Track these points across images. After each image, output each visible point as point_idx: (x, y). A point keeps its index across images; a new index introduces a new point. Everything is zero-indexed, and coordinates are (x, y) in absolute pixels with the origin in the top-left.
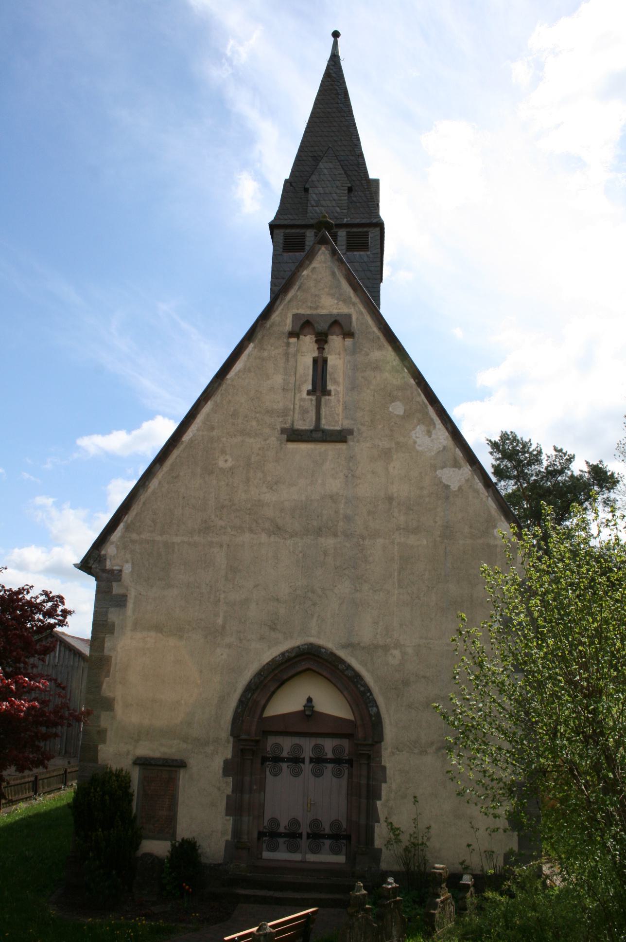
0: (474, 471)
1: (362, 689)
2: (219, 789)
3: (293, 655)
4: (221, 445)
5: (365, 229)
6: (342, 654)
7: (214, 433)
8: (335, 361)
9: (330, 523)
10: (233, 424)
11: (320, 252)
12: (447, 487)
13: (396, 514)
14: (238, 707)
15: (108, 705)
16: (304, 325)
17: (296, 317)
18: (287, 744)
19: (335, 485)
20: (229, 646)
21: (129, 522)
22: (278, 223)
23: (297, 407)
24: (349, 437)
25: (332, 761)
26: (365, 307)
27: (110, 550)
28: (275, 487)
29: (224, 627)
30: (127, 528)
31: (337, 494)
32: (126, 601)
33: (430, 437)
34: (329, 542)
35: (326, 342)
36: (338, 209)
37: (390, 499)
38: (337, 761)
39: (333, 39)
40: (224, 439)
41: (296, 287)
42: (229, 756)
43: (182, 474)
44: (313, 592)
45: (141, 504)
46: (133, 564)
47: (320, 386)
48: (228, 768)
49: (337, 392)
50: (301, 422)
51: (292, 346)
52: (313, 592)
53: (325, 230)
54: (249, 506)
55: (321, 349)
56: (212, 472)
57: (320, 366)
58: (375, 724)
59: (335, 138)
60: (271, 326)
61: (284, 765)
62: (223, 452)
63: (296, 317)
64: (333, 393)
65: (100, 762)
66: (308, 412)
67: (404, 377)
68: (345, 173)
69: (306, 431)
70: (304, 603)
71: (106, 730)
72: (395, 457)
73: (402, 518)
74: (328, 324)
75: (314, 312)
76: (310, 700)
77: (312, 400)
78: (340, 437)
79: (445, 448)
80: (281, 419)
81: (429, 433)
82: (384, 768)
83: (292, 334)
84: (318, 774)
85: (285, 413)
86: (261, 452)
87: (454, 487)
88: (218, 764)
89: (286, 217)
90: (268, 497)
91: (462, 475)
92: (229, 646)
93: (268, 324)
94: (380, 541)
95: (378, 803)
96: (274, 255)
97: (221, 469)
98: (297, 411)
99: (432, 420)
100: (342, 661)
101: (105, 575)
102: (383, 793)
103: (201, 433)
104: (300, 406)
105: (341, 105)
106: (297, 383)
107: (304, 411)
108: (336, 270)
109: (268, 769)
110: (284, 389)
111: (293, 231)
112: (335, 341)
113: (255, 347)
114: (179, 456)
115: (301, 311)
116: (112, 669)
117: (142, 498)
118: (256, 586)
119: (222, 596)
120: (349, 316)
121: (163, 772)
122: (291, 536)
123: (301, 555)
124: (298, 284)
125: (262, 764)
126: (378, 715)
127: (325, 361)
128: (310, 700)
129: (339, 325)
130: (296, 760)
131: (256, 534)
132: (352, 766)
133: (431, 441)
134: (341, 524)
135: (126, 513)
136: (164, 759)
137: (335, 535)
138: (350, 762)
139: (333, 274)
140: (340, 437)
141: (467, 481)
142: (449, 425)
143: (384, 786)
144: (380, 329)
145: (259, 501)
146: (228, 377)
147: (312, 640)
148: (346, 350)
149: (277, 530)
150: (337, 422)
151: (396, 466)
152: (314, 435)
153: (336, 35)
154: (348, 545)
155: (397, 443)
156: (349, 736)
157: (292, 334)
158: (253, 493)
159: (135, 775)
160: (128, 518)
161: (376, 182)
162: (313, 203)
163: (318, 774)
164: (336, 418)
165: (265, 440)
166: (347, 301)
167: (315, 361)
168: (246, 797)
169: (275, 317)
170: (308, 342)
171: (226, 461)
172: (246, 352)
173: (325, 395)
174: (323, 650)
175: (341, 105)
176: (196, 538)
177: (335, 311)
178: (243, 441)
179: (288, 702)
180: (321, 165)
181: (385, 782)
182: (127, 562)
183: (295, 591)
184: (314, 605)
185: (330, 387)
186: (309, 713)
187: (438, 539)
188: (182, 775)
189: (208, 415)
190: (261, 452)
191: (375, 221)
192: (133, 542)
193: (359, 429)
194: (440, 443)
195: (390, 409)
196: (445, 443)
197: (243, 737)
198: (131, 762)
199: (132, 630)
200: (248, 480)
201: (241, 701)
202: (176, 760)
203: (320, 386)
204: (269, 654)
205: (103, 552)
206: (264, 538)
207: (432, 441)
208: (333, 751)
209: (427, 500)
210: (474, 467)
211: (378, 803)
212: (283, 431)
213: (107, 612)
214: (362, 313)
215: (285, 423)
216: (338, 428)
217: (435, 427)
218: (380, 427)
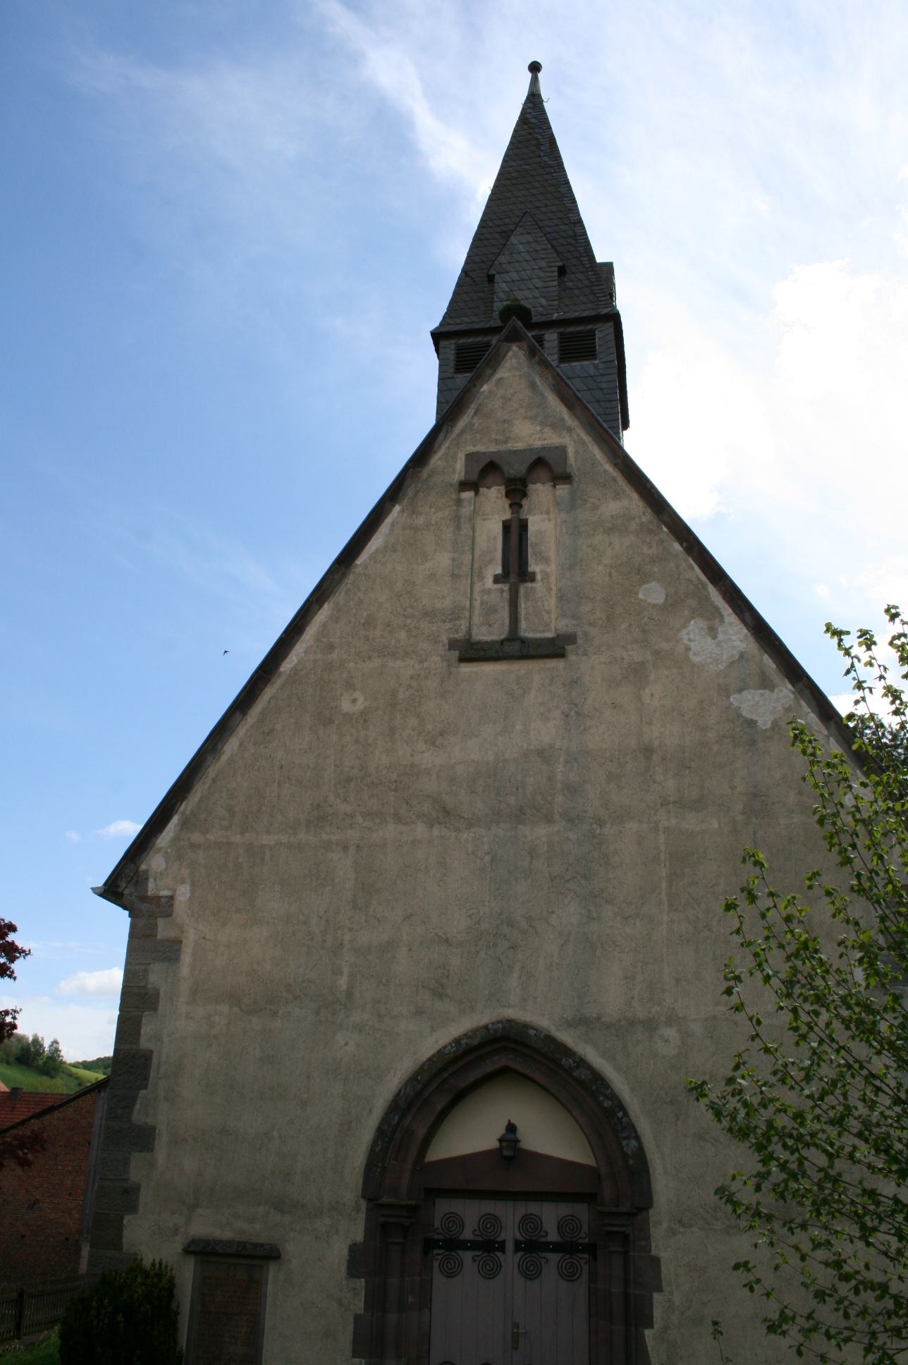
0: (800, 692)
1: (607, 1104)
2: (340, 1303)
3: (476, 1042)
4: (345, 675)
5: (589, 327)
6: (566, 1037)
7: (334, 656)
8: (543, 524)
9: (539, 798)
10: (367, 639)
11: (510, 353)
12: (751, 723)
13: (659, 778)
14: (375, 1143)
15: (144, 1139)
16: (486, 471)
17: (470, 457)
18: (471, 1214)
19: (546, 732)
20: (359, 1028)
21: (188, 813)
22: (446, 329)
23: (477, 604)
24: (569, 648)
25: (556, 1247)
26: (588, 433)
27: (155, 862)
28: (439, 741)
29: (349, 994)
30: (185, 824)
31: (551, 746)
32: (179, 950)
33: (714, 637)
34: (541, 832)
35: (524, 494)
36: (544, 302)
37: (647, 751)
38: (566, 1247)
39: (530, 75)
40: (351, 664)
41: (471, 411)
42: (360, 1237)
43: (279, 727)
44: (511, 924)
45: (209, 782)
46: (193, 884)
47: (516, 568)
48: (358, 1261)
49: (546, 575)
50: (484, 629)
51: (466, 504)
52: (511, 924)
53: (519, 323)
54: (394, 776)
55: (516, 506)
56: (331, 721)
57: (515, 533)
58: (636, 1171)
59: (537, 204)
60: (429, 476)
61: (467, 1256)
62: (350, 686)
63: (470, 457)
64: (539, 577)
65: (125, 1247)
66: (496, 611)
67: (662, 541)
68: (553, 247)
69: (493, 643)
70: (495, 945)
71: (139, 1186)
72: (652, 677)
73: (671, 783)
74: (526, 465)
75: (503, 448)
76: (511, 1128)
77: (502, 591)
78: (555, 649)
79: (742, 655)
80: (448, 625)
81: (712, 632)
82: (656, 1261)
83: (464, 485)
84: (531, 1273)
85: (455, 614)
86: (414, 684)
87: (764, 722)
88: (338, 1252)
89: (458, 321)
90: (430, 759)
91: (777, 700)
92: (359, 1028)
93: (425, 473)
94: (633, 826)
95: (648, 1333)
96: (441, 379)
97: (345, 715)
98: (476, 612)
99: (717, 609)
100: (568, 1052)
101: (144, 907)
102: (657, 1314)
103: (311, 657)
104: (482, 603)
105: (546, 159)
106: (476, 566)
107: (490, 610)
108: (537, 380)
109: (436, 1264)
110: (453, 576)
111: (471, 340)
112: (541, 492)
113: (403, 511)
114: (274, 697)
115: (480, 448)
116: (152, 1074)
117: (212, 771)
118: (408, 917)
119: (347, 937)
120: (563, 449)
121: (239, 1267)
122: (470, 826)
123: (487, 858)
124: (473, 406)
125: (426, 1253)
126: (640, 1154)
127: (524, 525)
128: (511, 1128)
129: (547, 466)
130: (488, 1246)
131: (407, 824)
132: (595, 1258)
133: (716, 646)
134: (560, 799)
135: (184, 798)
136: (239, 1243)
137: (549, 820)
138: (592, 1249)
139: (533, 386)
140: (555, 649)
141: (788, 710)
142: (748, 616)
143: (657, 1298)
144: (615, 465)
145: (412, 765)
146: (358, 562)
147: (511, 1013)
148: (558, 504)
149: (444, 814)
150: (547, 625)
151: (656, 693)
152: (506, 648)
153: (535, 68)
154: (572, 836)
155: (657, 653)
156: (589, 1198)
157: (464, 485)
158: (400, 753)
159: (186, 1275)
160: (186, 807)
161: (609, 267)
162: (502, 295)
163: (531, 1273)
164: (546, 617)
165: (422, 662)
166: (557, 425)
167: (506, 527)
168: (392, 1318)
169: (436, 460)
170: (494, 502)
171: (355, 701)
172: (388, 521)
173: (524, 581)
174: (532, 1032)
175: (546, 159)
176: (302, 836)
177: (538, 444)
178: (383, 666)
179: (471, 1134)
180: (513, 239)
181: (660, 1290)
182: (183, 882)
183: (478, 923)
184: (513, 948)
185: (534, 567)
186: (510, 1149)
187: (740, 818)
188: (273, 1273)
189: (324, 626)
190: (414, 684)
191: (604, 311)
192: (194, 847)
193: (585, 634)
194: (734, 648)
195: (641, 596)
196: (742, 646)
197: (385, 1200)
198: (180, 1250)
199: (189, 1003)
200: (392, 731)
201: (380, 1131)
202: (262, 1245)
203: (516, 568)
204: (433, 1042)
205: (143, 867)
206: (421, 830)
207: (719, 645)
208: (560, 1228)
209: (715, 748)
210: (800, 685)
211: (648, 1333)
212: (453, 644)
213: (146, 971)
214: (584, 443)
215: (456, 631)
216: (550, 635)
217: (722, 621)
218: (624, 626)
